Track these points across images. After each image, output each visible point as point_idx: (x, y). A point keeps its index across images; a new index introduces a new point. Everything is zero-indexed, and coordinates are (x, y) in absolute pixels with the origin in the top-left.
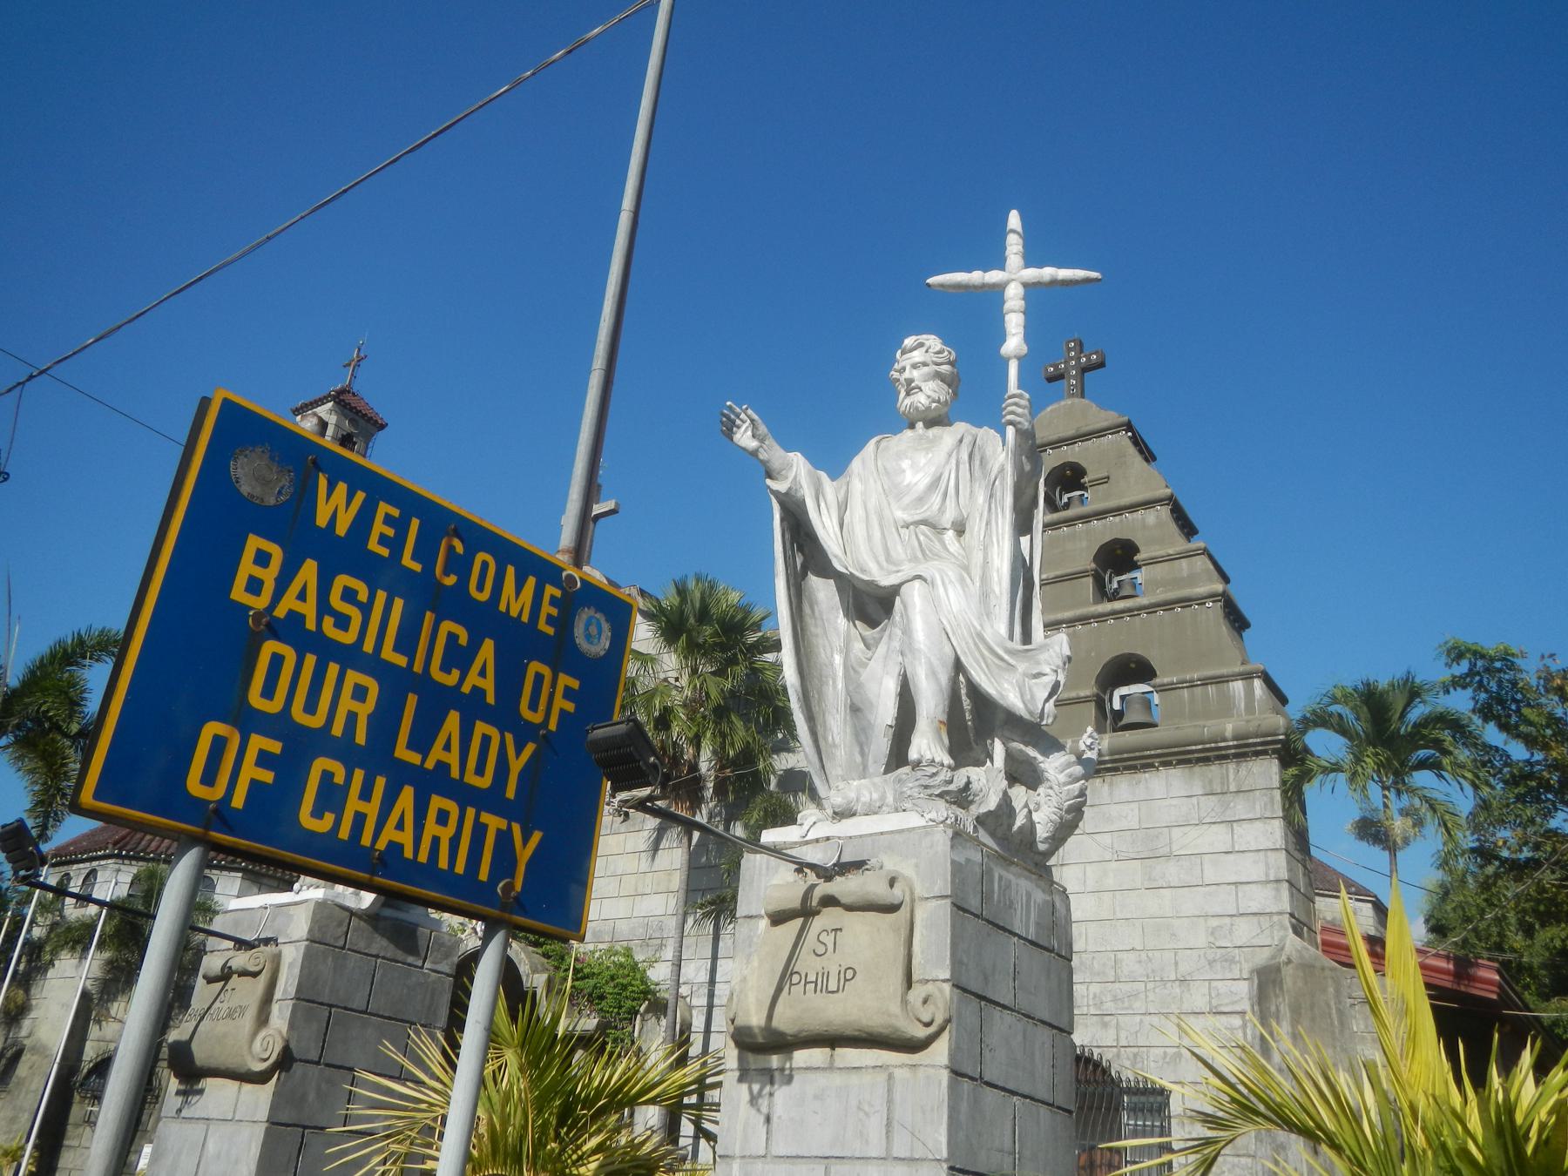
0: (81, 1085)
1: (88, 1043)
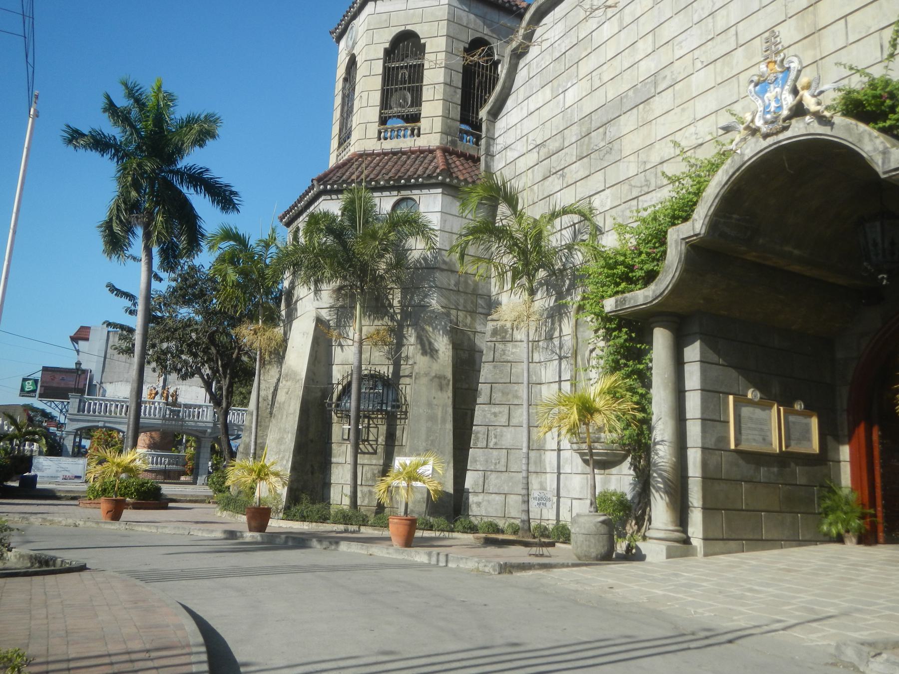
0: (337, 406)
1: (334, 367)
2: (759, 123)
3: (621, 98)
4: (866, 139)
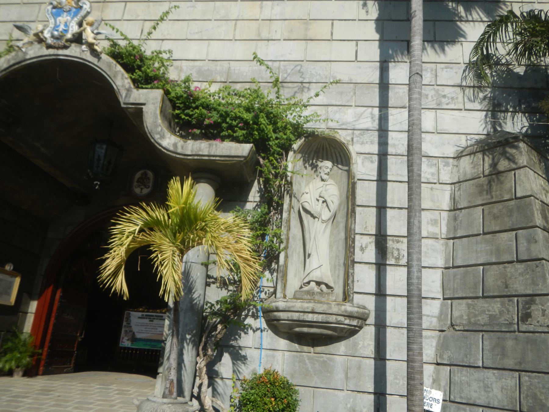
2: (47, 34)
4: (119, 77)
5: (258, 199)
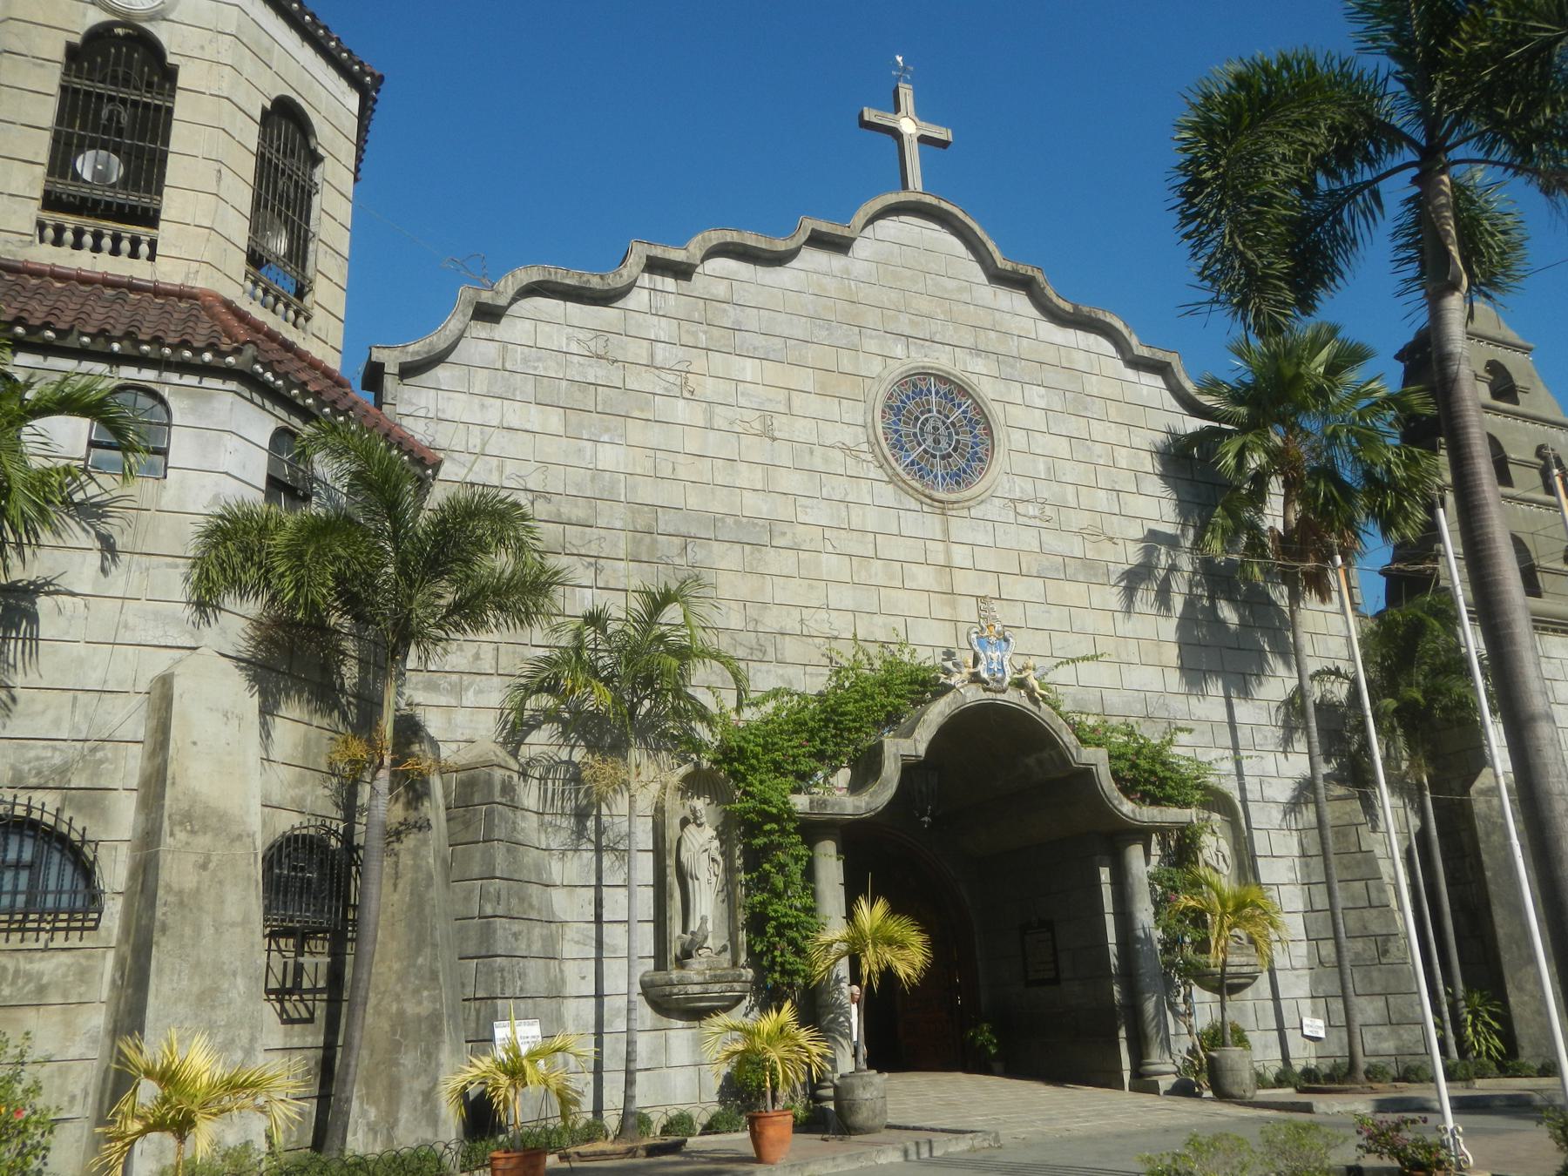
3: (716, 521)
4: (1064, 732)
5: (1159, 852)
